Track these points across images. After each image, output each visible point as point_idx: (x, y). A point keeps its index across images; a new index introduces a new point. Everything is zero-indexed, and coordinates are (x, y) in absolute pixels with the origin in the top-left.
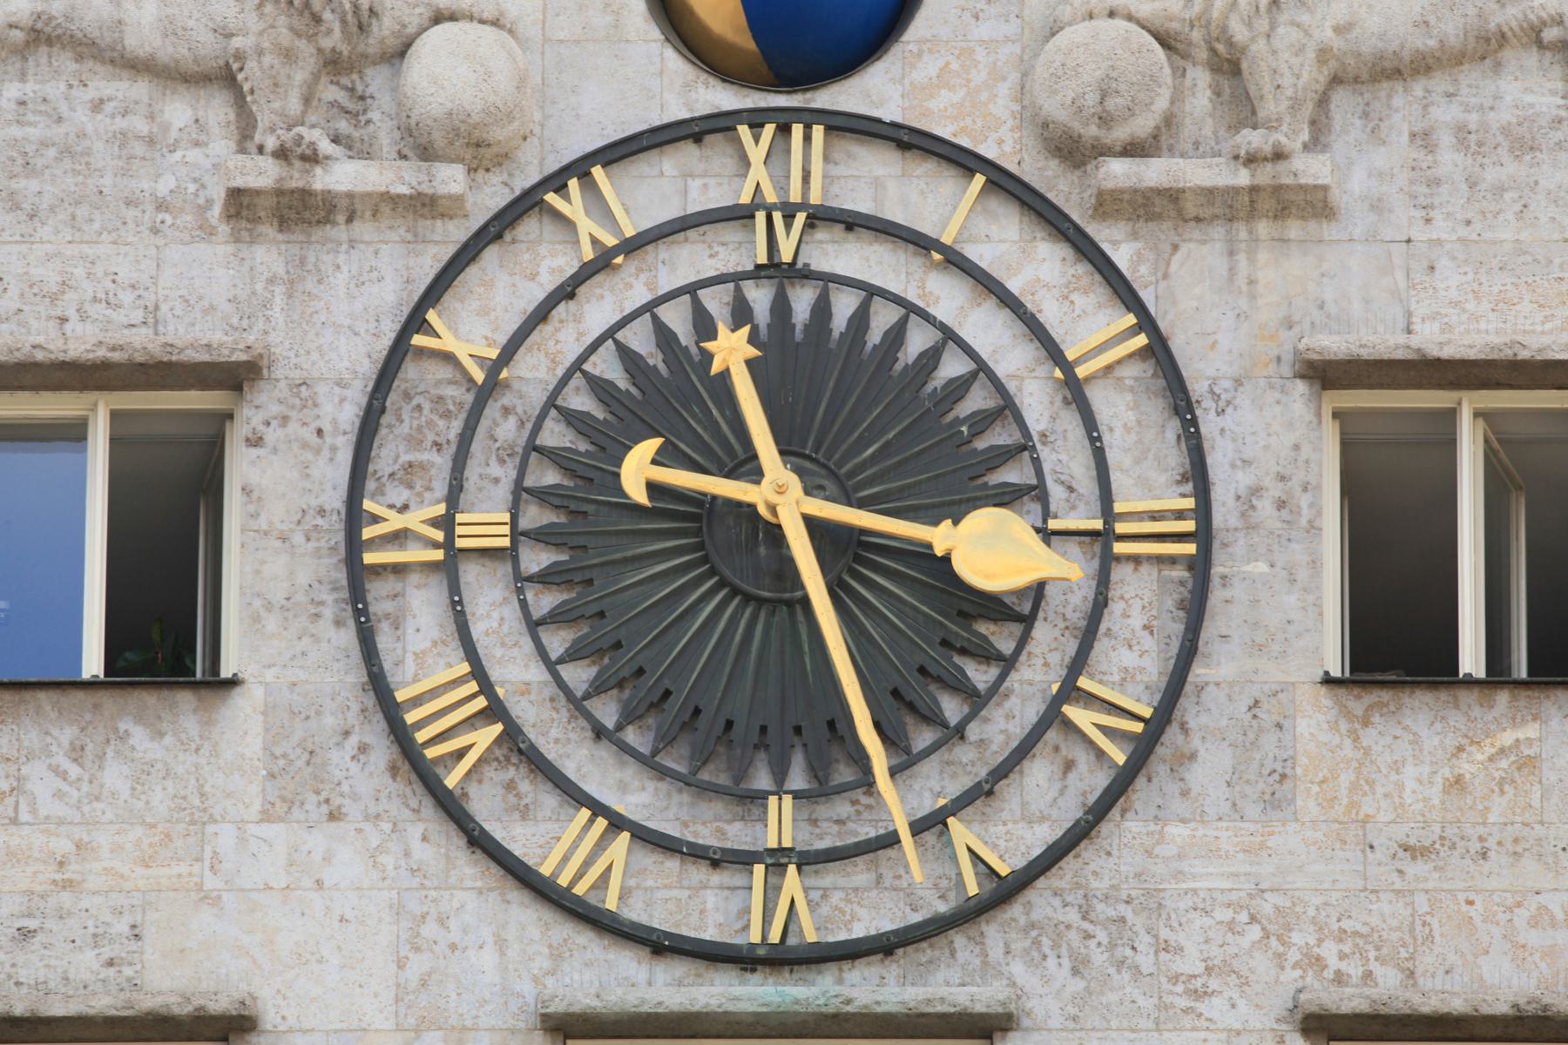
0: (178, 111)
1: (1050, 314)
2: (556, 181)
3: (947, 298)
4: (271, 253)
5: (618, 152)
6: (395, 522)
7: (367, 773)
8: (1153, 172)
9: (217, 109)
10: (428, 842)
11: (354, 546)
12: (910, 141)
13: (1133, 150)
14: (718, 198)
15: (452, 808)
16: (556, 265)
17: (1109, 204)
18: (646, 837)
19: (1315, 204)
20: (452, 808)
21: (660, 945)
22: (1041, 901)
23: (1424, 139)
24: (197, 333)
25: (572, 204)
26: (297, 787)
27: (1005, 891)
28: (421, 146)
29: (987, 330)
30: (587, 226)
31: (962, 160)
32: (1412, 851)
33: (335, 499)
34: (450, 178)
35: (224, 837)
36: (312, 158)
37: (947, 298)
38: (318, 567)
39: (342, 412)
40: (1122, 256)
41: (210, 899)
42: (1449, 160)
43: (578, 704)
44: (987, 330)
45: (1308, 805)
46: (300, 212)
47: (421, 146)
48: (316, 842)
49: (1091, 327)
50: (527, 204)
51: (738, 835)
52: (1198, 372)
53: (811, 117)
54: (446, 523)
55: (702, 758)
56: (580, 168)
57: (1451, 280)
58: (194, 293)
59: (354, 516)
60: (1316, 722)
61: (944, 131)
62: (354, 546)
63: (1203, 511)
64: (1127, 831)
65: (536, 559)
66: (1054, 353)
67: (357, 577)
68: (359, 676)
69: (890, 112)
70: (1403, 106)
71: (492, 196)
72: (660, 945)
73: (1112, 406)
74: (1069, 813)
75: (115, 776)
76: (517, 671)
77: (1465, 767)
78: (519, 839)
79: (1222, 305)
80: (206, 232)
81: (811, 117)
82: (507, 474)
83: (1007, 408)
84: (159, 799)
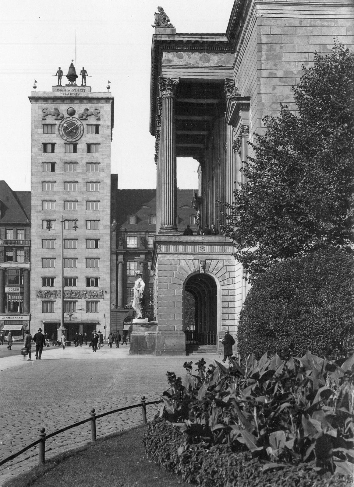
5: (66, 118)
10: (61, 138)
26: (57, 136)
58: (54, 122)
76: (63, 133)
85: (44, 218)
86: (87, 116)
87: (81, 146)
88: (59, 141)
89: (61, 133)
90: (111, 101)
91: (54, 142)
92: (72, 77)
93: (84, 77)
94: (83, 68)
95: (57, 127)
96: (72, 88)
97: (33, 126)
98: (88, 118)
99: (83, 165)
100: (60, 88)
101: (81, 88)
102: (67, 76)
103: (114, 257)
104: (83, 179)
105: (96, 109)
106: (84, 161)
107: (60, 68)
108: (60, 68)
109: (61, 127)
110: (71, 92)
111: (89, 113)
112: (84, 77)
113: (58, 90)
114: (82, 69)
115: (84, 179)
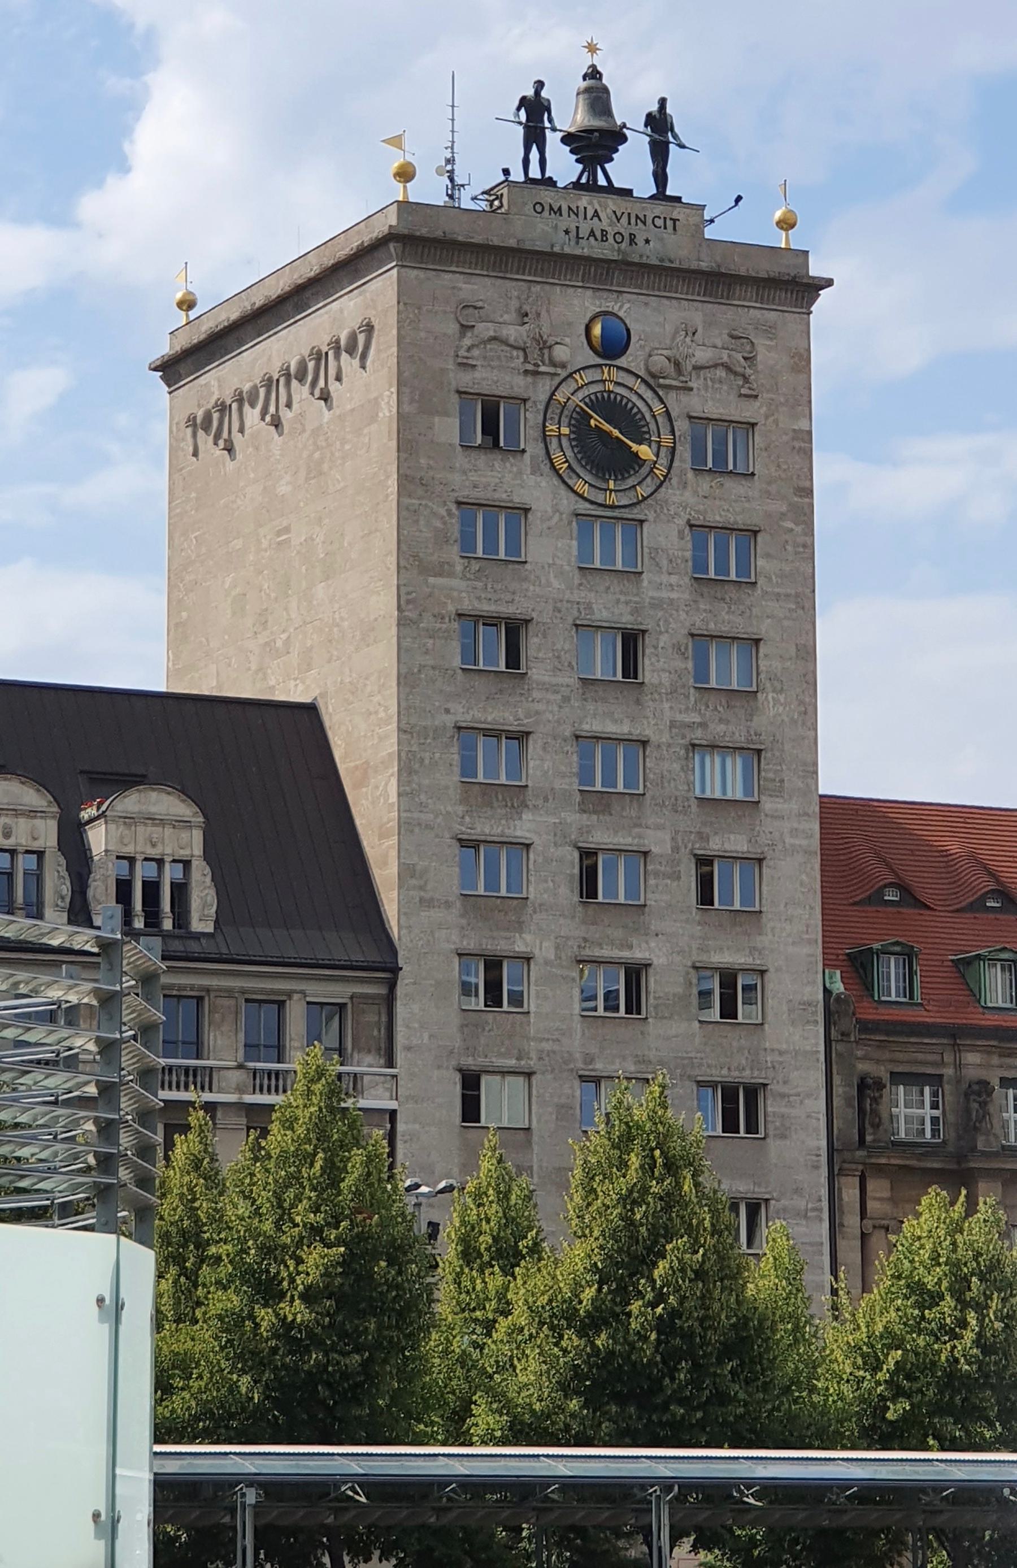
0: (515, 353)
1: (650, 402)
2: (575, 372)
3: (634, 398)
5: (583, 369)
6: (551, 427)
7: (546, 468)
8: (667, 382)
9: (521, 354)
10: (556, 481)
11: (544, 431)
13: (663, 378)
14: (599, 378)
15: (560, 476)
16: (574, 386)
17: (660, 386)
18: (590, 485)
20: (560, 476)
21: (592, 503)
22: (650, 501)
23: (705, 379)
24: (519, 391)
25: (577, 376)
26: (535, 470)
28: (553, 364)
29: (640, 404)
30: (580, 381)
31: (638, 376)
32: (705, 497)
33: (541, 422)
34: (559, 371)
35: (525, 477)
36: (539, 366)
37: (634, 398)
38: (536, 433)
39: (541, 407)
40: (661, 393)
41: (523, 487)
42: (710, 383)
43: (579, 461)
44: (640, 404)
45: (690, 488)
47: (553, 364)
48: (539, 479)
49: (658, 408)
50: (570, 375)
51: (604, 486)
52: (673, 414)
53: (614, 366)
54: (559, 428)
55: (597, 472)
56: (578, 370)
57: (710, 403)
58: (519, 385)
59: (544, 426)
60: (690, 475)
61: (633, 370)
62: (544, 431)
63: (674, 439)
64: (663, 489)
65: (572, 436)
66: (651, 410)
67: (545, 436)
68: (544, 451)
69: (625, 366)
71: (564, 374)
72: (592, 503)
73: (660, 419)
74: (654, 487)
75: (508, 465)
77: (713, 484)
78: (570, 482)
79: (677, 404)
80: (519, 374)
81: (614, 366)
82: (567, 420)
83: (644, 417)
84: (515, 469)
85: (470, 944)
87: (665, 535)
89: (557, 456)
92: (596, 144)
93: (660, 153)
94: (663, 102)
96: (613, 203)
97: (406, 399)
99: (677, 648)
100: (547, 196)
101: (660, 209)
102: (568, 139)
104: (673, 724)
109: (554, 411)
110: (605, 224)
111: (702, 355)
112: (660, 153)
113: (539, 207)
114: (654, 108)
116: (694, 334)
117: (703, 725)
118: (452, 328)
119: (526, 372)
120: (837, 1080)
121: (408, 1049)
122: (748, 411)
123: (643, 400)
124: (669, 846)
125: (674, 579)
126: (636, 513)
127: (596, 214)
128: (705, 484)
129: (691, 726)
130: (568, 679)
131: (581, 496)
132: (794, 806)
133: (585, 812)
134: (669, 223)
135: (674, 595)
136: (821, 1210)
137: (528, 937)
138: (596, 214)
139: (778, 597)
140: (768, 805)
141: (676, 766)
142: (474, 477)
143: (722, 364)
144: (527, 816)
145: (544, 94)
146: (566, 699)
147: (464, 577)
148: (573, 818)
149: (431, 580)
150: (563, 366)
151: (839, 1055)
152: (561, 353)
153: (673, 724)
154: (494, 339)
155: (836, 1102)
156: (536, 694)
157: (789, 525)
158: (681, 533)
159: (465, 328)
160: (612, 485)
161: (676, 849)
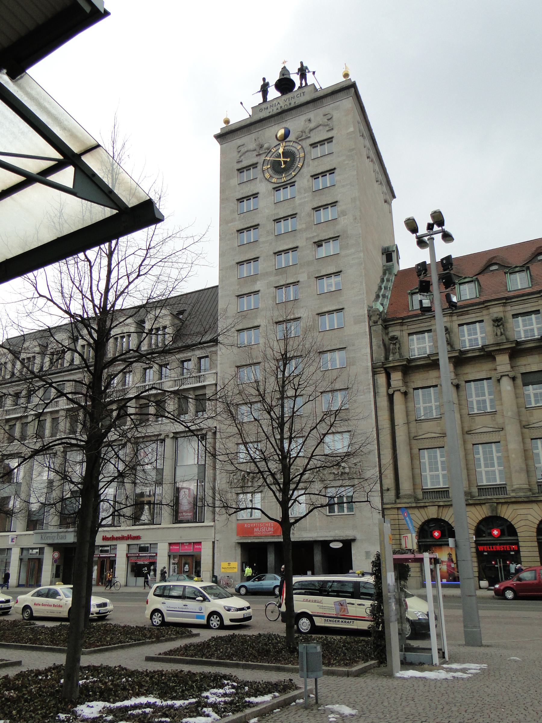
0: (254, 152)
3: (292, 148)
4: (258, 157)
7: (264, 180)
10: (267, 182)
12: (289, 141)
17: (299, 141)
19: (309, 137)
26: (261, 181)
27: (295, 175)
46: (259, 155)
47: (265, 150)
60: (311, 162)
70: (314, 131)
76: (271, 172)
86: (311, 130)
88: (263, 187)
90: (353, 90)
91: (255, 192)
94: (302, 63)
95: (259, 167)
98: (312, 134)
103: (382, 379)
104: (307, 239)
105: (325, 115)
106: (308, 208)
107: (264, 79)
108: (264, 79)
111: (312, 125)
115: (311, 238)
116: (310, 120)
117: (318, 235)
118: (236, 153)
119: (257, 155)
120: (373, 340)
121: (221, 364)
122: (329, 135)
123: (296, 148)
124: (306, 278)
125: (306, 195)
126: (293, 180)
127: (278, 103)
128: (316, 162)
129: (313, 237)
130: (272, 237)
131: (274, 183)
132: (353, 250)
133: (277, 276)
134: (302, 94)
135: (307, 199)
136: (370, 389)
137: (259, 320)
138: (278, 103)
139: (343, 186)
140: (343, 253)
141: (308, 252)
142: (242, 191)
143: (320, 125)
144: (258, 283)
145: (266, 81)
146: (271, 244)
147: (239, 220)
148: (273, 279)
149: (229, 225)
150: (268, 149)
151: (374, 331)
152: (266, 146)
153: (307, 239)
154: (247, 151)
155: (374, 348)
156: (261, 246)
157: (347, 162)
158: (308, 181)
159: (239, 152)
160: (284, 175)
161: (309, 278)
